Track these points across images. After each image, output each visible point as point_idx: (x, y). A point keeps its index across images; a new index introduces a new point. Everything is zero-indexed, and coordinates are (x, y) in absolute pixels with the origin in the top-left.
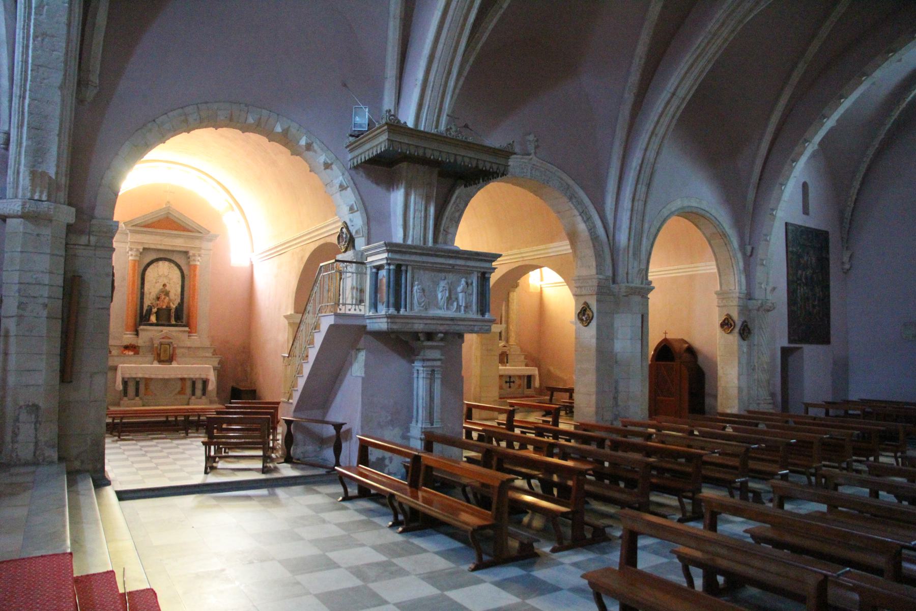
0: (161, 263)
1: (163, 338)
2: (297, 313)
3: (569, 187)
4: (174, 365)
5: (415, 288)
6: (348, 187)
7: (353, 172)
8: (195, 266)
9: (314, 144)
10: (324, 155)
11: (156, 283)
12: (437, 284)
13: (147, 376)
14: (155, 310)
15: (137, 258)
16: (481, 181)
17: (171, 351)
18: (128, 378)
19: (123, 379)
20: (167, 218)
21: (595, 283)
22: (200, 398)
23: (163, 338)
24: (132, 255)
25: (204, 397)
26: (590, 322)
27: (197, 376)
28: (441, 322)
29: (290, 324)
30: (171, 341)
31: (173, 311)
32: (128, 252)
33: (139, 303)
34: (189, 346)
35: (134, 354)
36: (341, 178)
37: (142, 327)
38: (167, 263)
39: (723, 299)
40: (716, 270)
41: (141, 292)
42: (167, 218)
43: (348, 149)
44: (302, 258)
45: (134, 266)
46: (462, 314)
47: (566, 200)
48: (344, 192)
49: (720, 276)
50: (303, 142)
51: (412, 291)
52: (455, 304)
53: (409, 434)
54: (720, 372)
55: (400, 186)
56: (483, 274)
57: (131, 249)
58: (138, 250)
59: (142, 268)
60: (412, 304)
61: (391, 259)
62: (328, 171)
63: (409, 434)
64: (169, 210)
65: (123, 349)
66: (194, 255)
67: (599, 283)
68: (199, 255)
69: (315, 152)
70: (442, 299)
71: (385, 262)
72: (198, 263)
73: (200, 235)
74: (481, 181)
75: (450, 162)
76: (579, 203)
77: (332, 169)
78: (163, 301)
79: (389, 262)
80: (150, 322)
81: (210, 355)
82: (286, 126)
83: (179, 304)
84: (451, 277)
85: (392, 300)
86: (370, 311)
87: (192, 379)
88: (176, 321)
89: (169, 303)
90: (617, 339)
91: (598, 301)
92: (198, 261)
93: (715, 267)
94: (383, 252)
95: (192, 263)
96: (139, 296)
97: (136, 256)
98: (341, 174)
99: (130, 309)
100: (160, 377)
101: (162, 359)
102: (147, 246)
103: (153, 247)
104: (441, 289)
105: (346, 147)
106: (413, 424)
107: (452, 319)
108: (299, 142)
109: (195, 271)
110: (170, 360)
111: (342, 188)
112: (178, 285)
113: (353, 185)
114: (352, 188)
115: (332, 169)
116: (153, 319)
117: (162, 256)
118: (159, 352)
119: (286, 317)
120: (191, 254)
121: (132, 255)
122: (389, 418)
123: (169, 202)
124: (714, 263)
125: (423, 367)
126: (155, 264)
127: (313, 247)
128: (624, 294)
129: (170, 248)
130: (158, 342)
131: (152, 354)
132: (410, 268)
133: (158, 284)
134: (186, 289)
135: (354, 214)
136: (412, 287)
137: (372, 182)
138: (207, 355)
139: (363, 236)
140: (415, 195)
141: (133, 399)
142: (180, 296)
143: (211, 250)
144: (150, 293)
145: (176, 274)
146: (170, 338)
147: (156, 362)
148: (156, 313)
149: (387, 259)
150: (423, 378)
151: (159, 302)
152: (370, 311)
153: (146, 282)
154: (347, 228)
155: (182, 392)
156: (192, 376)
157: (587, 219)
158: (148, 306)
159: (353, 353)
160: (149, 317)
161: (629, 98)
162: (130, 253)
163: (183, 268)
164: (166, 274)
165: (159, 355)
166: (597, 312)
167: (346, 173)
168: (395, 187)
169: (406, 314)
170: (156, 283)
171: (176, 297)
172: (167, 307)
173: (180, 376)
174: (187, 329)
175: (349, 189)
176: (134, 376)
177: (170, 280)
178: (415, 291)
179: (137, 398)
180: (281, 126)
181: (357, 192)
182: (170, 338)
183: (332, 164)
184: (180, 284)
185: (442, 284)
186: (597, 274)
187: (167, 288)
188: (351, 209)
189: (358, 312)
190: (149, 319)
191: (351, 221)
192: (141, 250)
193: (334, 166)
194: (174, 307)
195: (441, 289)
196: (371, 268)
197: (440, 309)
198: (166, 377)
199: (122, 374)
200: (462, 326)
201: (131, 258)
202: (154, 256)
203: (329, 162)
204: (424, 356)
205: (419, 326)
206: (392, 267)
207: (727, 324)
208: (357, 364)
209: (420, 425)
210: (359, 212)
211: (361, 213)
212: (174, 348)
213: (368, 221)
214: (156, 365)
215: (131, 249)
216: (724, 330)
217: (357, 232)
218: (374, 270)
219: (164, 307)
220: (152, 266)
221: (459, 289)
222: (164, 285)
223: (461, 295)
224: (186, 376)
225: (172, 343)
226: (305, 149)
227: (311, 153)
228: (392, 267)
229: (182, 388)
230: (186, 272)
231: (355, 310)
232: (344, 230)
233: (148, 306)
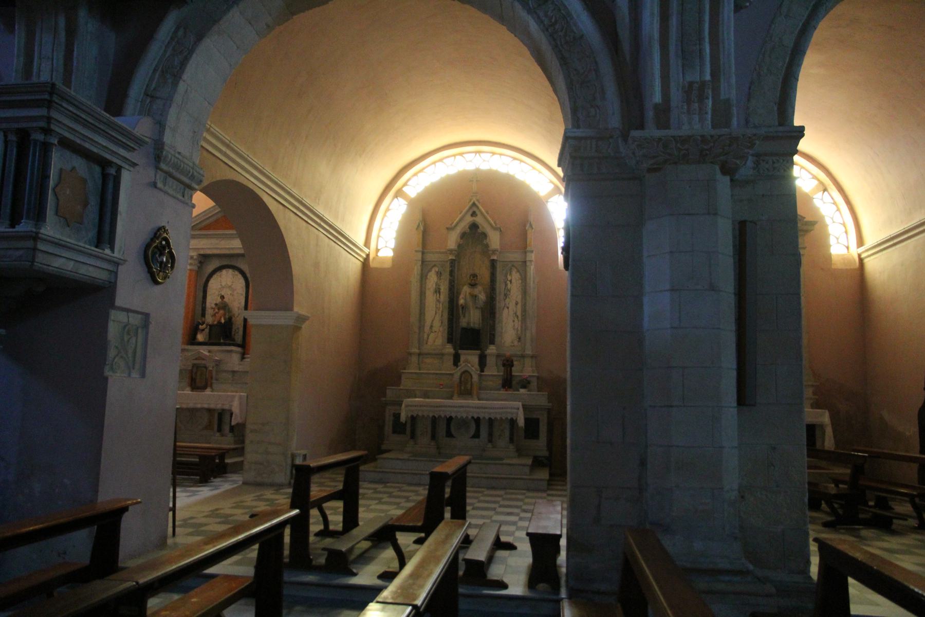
0: (224, 272)
1: (196, 359)
4: (208, 392)
15: (195, 268)
23: (196, 359)
38: (230, 271)
41: (202, 307)
45: (190, 276)
102: (202, 252)
110: (204, 388)
116: (200, 337)
117: (225, 262)
126: (218, 273)
129: (227, 252)
145: (240, 283)
147: (188, 388)
155: (209, 427)
163: (248, 275)
164: (229, 284)
177: (233, 291)
182: (203, 359)
184: (244, 295)
201: (189, 267)
202: (214, 264)
214: (188, 391)
220: (215, 276)
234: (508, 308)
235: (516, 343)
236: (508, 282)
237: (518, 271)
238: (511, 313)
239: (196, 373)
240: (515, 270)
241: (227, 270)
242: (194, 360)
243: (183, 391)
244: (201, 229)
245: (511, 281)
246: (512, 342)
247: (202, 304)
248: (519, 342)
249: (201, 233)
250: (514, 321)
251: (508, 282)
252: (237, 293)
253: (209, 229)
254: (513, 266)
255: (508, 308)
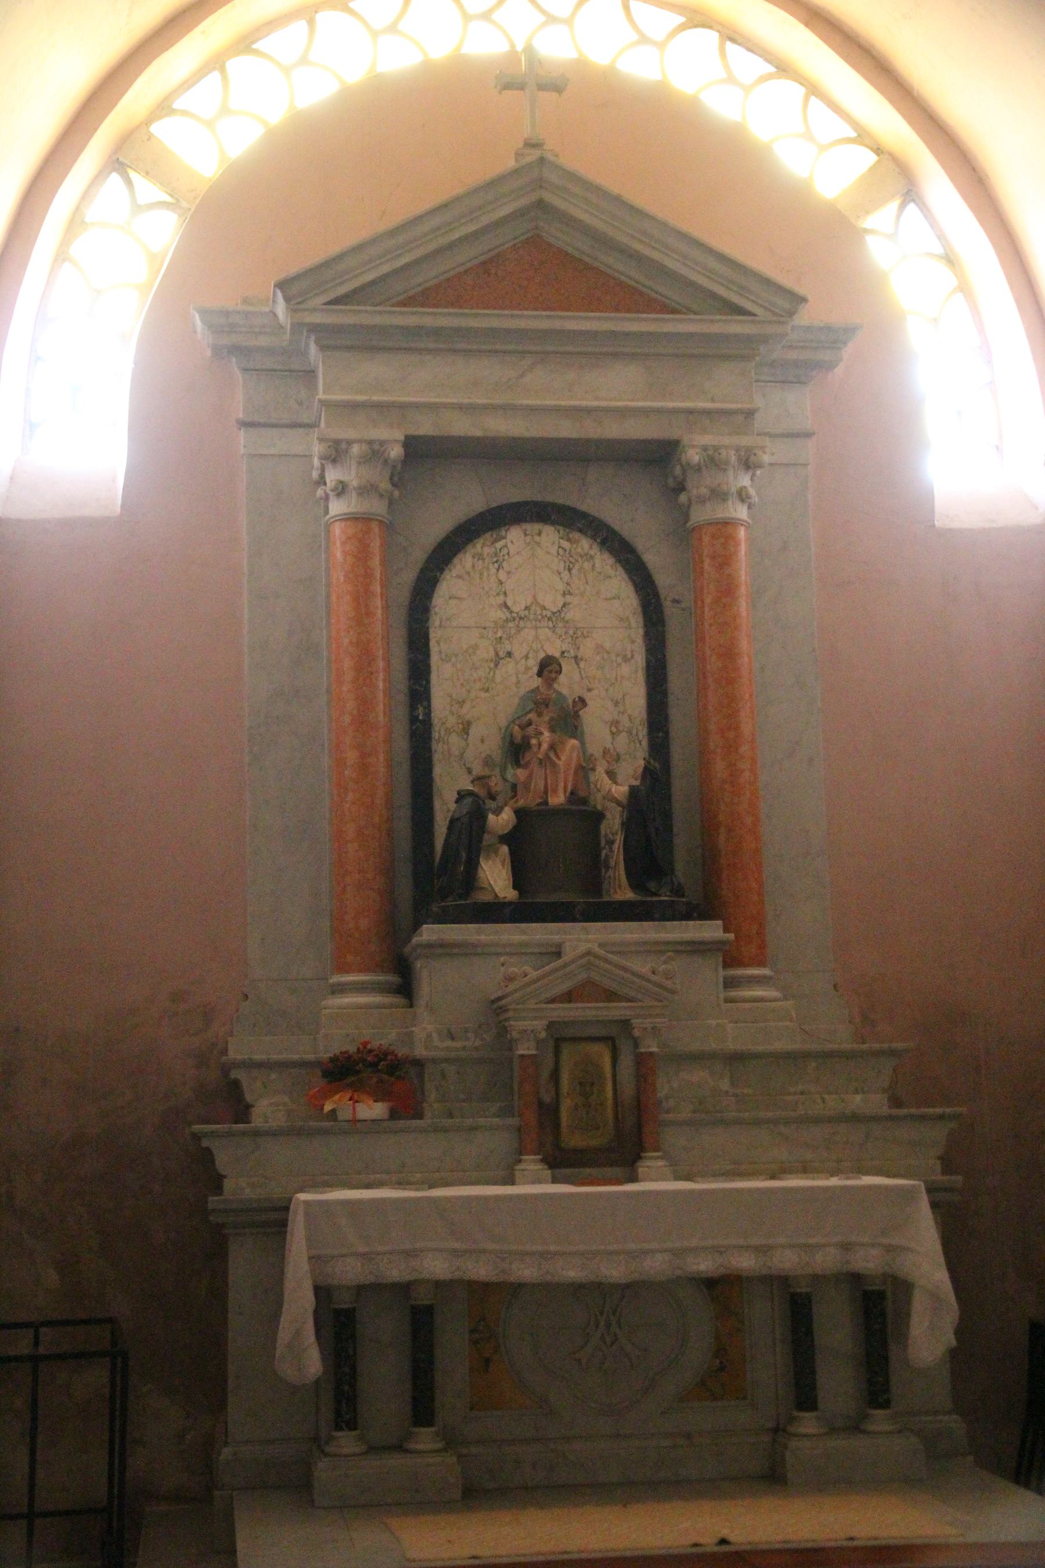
0: (515, 537)
1: (569, 997)
8: (725, 528)
11: (497, 661)
13: (481, 1271)
14: (502, 820)
15: (378, 507)
17: (628, 1089)
18: (360, 1290)
19: (322, 1292)
20: (535, 242)
22: (856, 1427)
23: (569, 997)
24: (341, 489)
25: (880, 1420)
27: (826, 1260)
30: (616, 1011)
31: (613, 824)
32: (322, 481)
33: (403, 797)
34: (731, 1046)
35: (393, 1115)
37: (429, 933)
38: (550, 536)
41: (413, 720)
42: (535, 242)
45: (362, 555)
57: (336, 453)
58: (374, 453)
59: (408, 577)
64: (540, 183)
65: (319, 1082)
66: (714, 461)
68: (748, 464)
72: (741, 512)
73: (737, 327)
78: (546, 762)
80: (484, 897)
81: (877, 1103)
83: (647, 771)
87: (783, 1281)
88: (636, 882)
89: (584, 769)
92: (742, 496)
95: (699, 515)
96: (402, 744)
97: (365, 490)
99: (350, 830)
100: (572, 1273)
101: (573, 1140)
102: (425, 427)
103: (462, 427)
109: (724, 561)
112: (625, 669)
118: (547, 1098)
120: (694, 456)
121: (341, 489)
123: (531, 144)
126: (482, 546)
129: (566, 429)
130: (540, 1025)
131: (507, 1111)
133: (508, 667)
134: (677, 680)
138: (856, 1101)
141: (399, 1448)
142: (643, 732)
143: (808, 435)
144: (466, 728)
146: (611, 996)
147: (531, 1164)
148: (511, 838)
151: (521, 774)
153: (434, 659)
156: (786, 1261)
158: (461, 796)
160: (473, 865)
162: (333, 475)
164: (551, 601)
165: (549, 1113)
170: (497, 661)
171: (622, 739)
172: (574, 797)
173: (705, 1265)
174: (711, 930)
176: (395, 1272)
179: (425, 1439)
182: (611, 996)
184: (640, 659)
187: (568, 684)
190: (470, 880)
192: (396, 452)
194: (620, 791)
198: (614, 1272)
199: (314, 1259)
201: (337, 507)
212: (644, 1065)
215: (336, 453)
219: (558, 799)
220: (465, 561)
222: (548, 668)
224: (746, 1263)
225: (625, 1024)
229: (720, 1352)
230: (663, 580)
233: (461, 796)
239: (555, 1076)
241: (534, 527)
242: (553, 1001)
243: (511, 1181)
244: (425, 298)
247: (413, 707)
249: (428, 321)
252: (599, 648)
253: (405, 305)
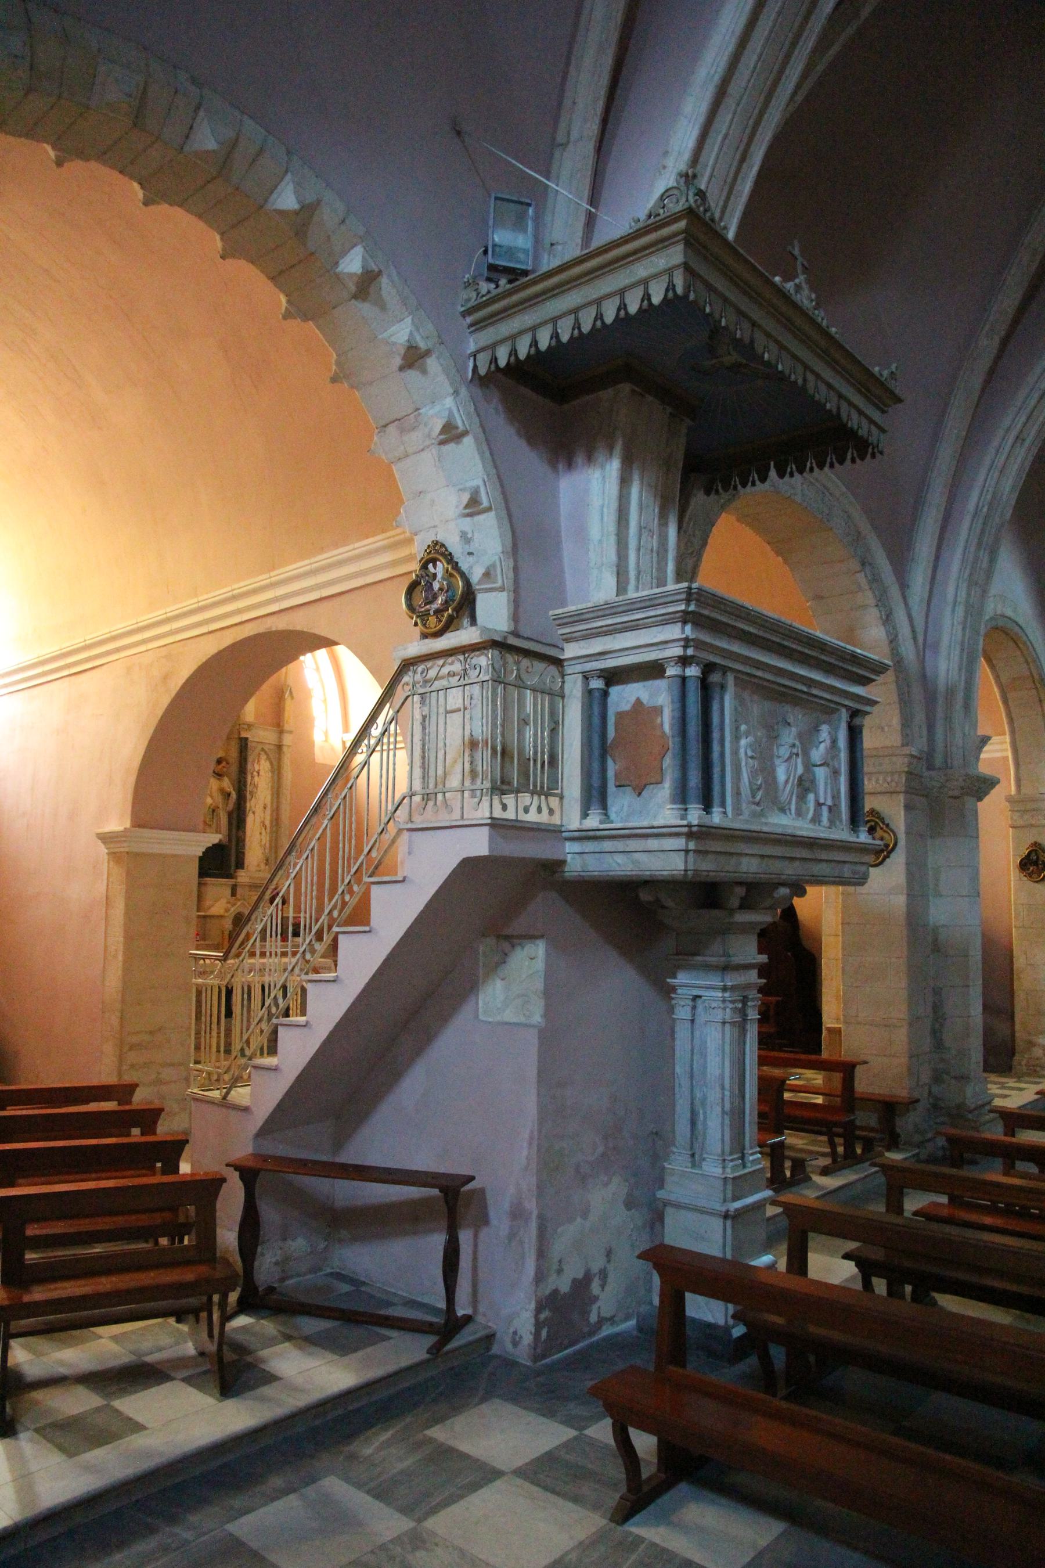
2: (139, 826)
3: (858, 538)
5: (743, 742)
6: (465, 433)
7: (478, 391)
9: (384, 281)
10: (409, 320)
12: (773, 737)
16: (773, 473)
21: (901, 764)
26: (888, 856)
28: (788, 852)
29: (115, 857)
36: (449, 402)
39: (1026, 811)
40: (1009, 754)
43: (469, 320)
44: (166, 678)
46: (822, 832)
47: (854, 565)
48: (451, 447)
49: (1017, 764)
50: (353, 264)
51: (735, 752)
52: (811, 797)
53: (661, 1194)
54: (1019, 962)
55: (600, 456)
56: (854, 714)
60: (738, 794)
61: (699, 644)
62: (412, 375)
63: (661, 1194)
67: (910, 764)
69: (383, 307)
70: (787, 782)
71: (677, 651)
74: (773, 473)
75: (795, 382)
76: (875, 580)
77: (424, 372)
79: (690, 652)
82: (310, 198)
84: (798, 719)
85: (694, 779)
86: (585, 815)
90: (938, 895)
91: (908, 807)
93: (1008, 746)
94: (666, 621)
98: (451, 391)
104: (784, 751)
105: (465, 314)
106: (678, 1163)
107: (812, 843)
108: (337, 263)
111: (450, 434)
113: (479, 430)
114: (476, 439)
115: (424, 372)
119: (105, 838)
122: (601, 1149)
124: (1007, 738)
125: (725, 989)
127: (210, 648)
128: (956, 793)
132: (730, 679)
135: (477, 518)
136: (737, 738)
137: (518, 433)
139: (502, 589)
140: (642, 483)
149: (687, 642)
150: (724, 1023)
152: (585, 815)
154: (450, 558)
157: (888, 619)
159: (485, 946)
161: (988, 344)
166: (907, 833)
167: (464, 392)
168: (580, 459)
169: (725, 825)
175: (468, 441)
178: (742, 751)
180: (296, 192)
181: (487, 454)
183: (428, 353)
185: (789, 737)
186: (903, 745)
188: (473, 506)
189: (544, 818)
191: (465, 538)
193: (432, 363)
195: (784, 751)
196: (586, 677)
197: (783, 810)
200: (824, 865)
203: (422, 345)
204: (726, 954)
205: (750, 866)
206: (693, 671)
207: (1036, 863)
208: (499, 984)
209: (713, 1168)
210: (492, 514)
211: (499, 518)
213: (515, 549)
216: (1030, 875)
217: (487, 575)
218: (597, 684)
221: (818, 754)
223: (821, 773)
226: (353, 288)
227: (366, 309)
228: (693, 671)
231: (539, 810)
232: (439, 569)
234: (254, 813)
235: (263, 866)
236: (255, 773)
237: (268, 758)
238: (258, 820)
240: (265, 757)
245: (258, 773)
246: (258, 865)
248: (266, 864)
250: (261, 833)
251: (255, 773)
254: (263, 750)
255: (254, 813)
